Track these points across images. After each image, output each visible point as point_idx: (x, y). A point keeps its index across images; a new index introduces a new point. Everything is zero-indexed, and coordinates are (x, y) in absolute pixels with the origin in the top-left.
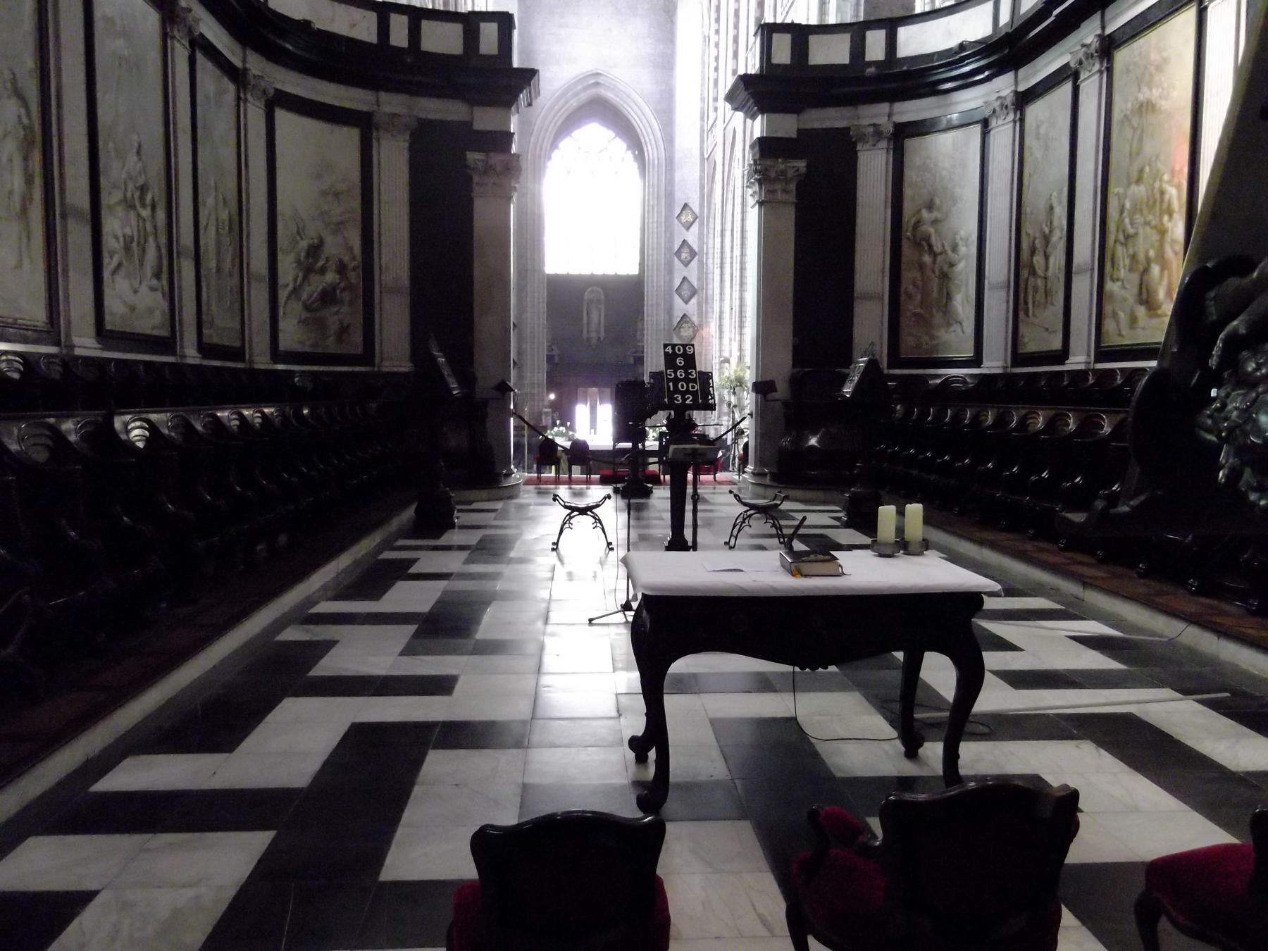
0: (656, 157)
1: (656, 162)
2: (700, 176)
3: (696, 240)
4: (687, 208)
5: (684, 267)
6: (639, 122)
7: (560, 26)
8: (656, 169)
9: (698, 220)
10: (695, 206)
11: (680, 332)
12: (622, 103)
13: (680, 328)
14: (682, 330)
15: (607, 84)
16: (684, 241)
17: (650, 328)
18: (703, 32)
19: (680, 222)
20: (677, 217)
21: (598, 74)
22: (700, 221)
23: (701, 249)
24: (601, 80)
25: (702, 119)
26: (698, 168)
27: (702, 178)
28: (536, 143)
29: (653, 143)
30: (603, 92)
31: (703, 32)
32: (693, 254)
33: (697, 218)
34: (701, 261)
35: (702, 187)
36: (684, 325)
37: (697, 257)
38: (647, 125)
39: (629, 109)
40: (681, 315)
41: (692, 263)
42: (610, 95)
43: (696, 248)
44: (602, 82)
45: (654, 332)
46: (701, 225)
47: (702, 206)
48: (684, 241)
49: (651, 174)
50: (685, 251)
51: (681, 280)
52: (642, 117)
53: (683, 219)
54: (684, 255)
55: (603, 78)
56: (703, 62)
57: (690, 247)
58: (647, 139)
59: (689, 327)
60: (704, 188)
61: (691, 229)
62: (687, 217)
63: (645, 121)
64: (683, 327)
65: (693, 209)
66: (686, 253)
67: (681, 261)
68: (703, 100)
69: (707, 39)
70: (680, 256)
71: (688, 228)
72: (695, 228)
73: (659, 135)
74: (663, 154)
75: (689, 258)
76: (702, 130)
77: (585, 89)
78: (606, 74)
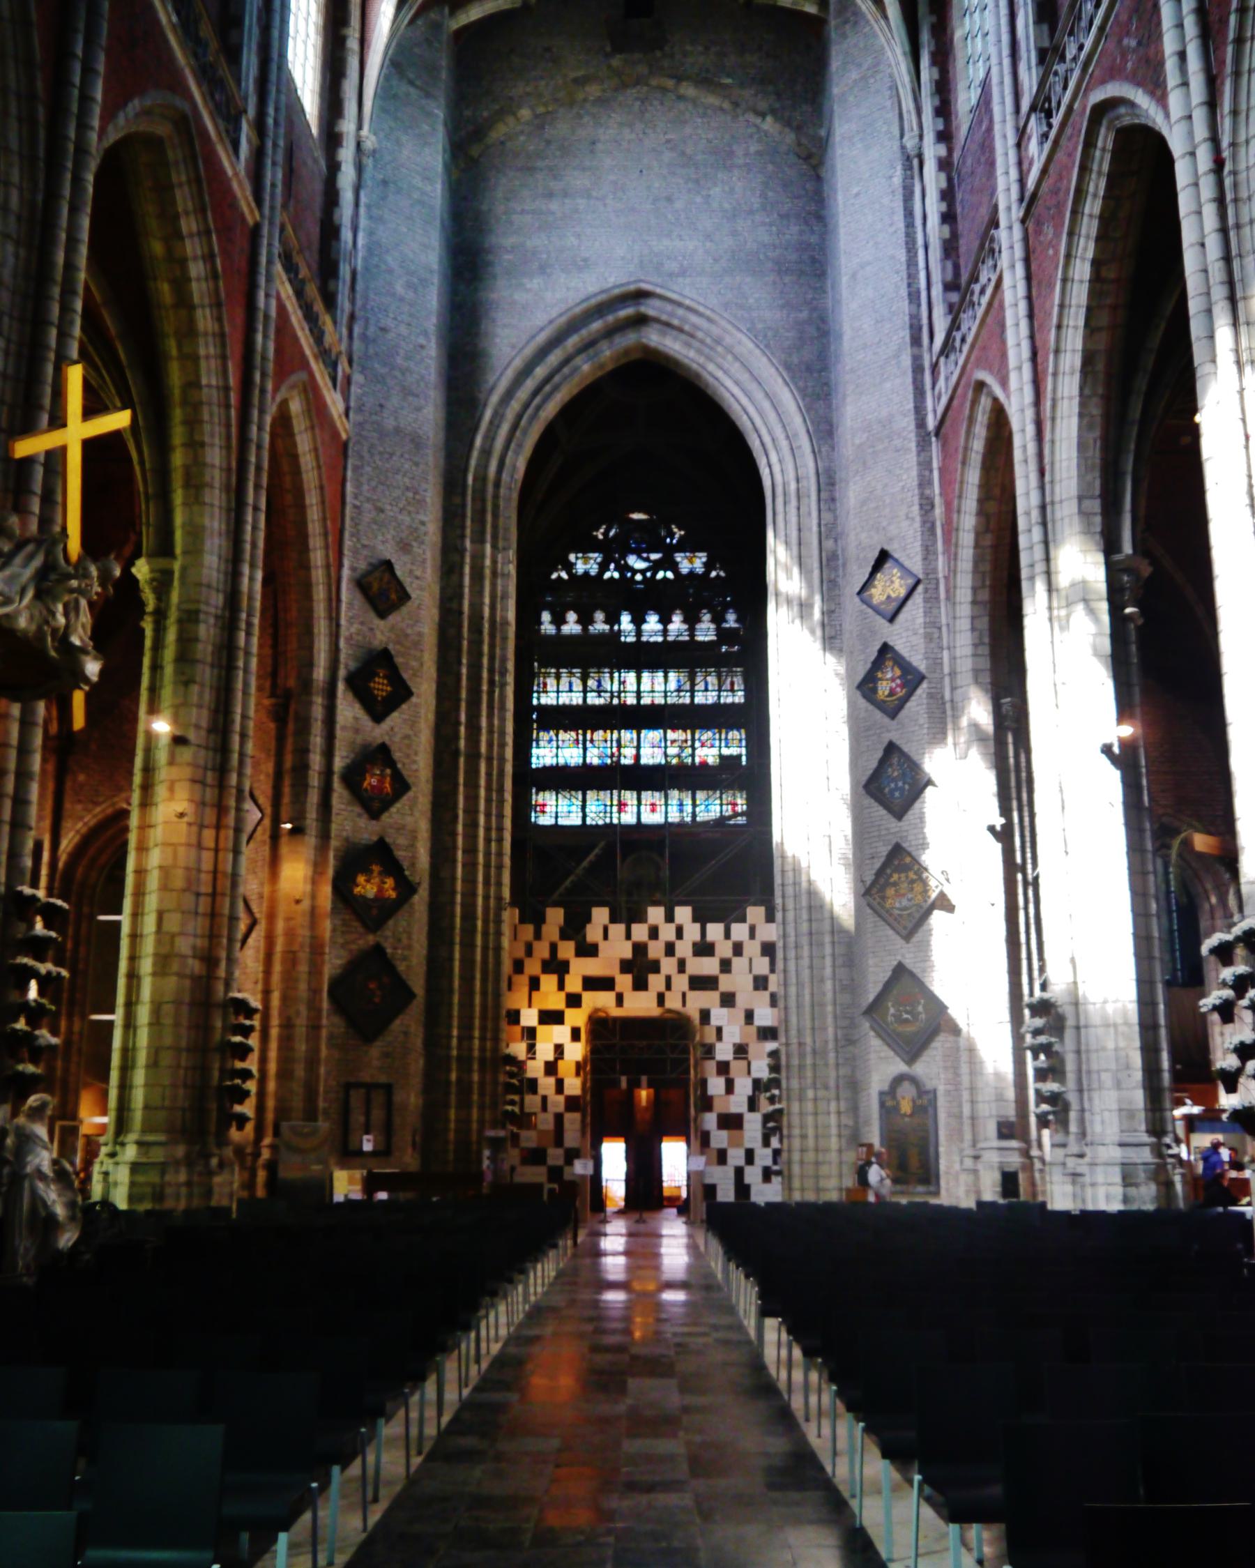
0: (791, 475)
1: (793, 486)
2: (921, 476)
3: (919, 641)
4: (888, 565)
5: (886, 720)
6: (744, 401)
7: (550, 195)
8: (794, 503)
9: (920, 588)
10: (910, 553)
11: (884, 898)
12: (702, 360)
13: (882, 890)
14: (890, 892)
15: (664, 317)
16: (885, 649)
17: (790, 904)
18: (903, 147)
19: (870, 605)
20: (859, 593)
21: (641, 295)
22: (926, 591)
23: (936, 663)
24: (650, 308)
25: (916, 341)
26: (912, 458)
27: (924, 483)
28: (486, 453)
29: (784, 444)
30: (654, 338)
31: (903, 147)
32: (912, 679)
33: (918, 582)
34: (936, 698)
35: (927, 506)
36: (895, 876)
37: (924, 685)
38: (766, 405)
39: (720, 374)
40: (884, 850)
41: (909, 705)
42: (672, 345)
43: (918, 661)
44: (651, 312)
45: (805, 916)
46: (932, 601)
47: (928, 552)
48: (885, 649)
49: (780, 518)
50: (889, 675)
51: (879, 754)
52: (753, 387)
53: (878, 593)
54: (883, 688)
55: (657, 303)
56: (909, 213)
57: (900, 662)
58: (767, 439)
59: (913, 882)
60: (933, 506)
61: (902, 617)
62: (890, 585)
63: (759, 396)
64: (895, 884)
65: (907, 563)
66: (893, 680)
67: (880, 705)
68: (914, 297)
69: (912, 162)
70: (875, 690)
71: (892, 619)
72: (915, 611)
73: (798, 420)
74: (811, 465)
75: (901, 693)
76: (918, 369)
77: (610, 333)
78: (659, 290)
